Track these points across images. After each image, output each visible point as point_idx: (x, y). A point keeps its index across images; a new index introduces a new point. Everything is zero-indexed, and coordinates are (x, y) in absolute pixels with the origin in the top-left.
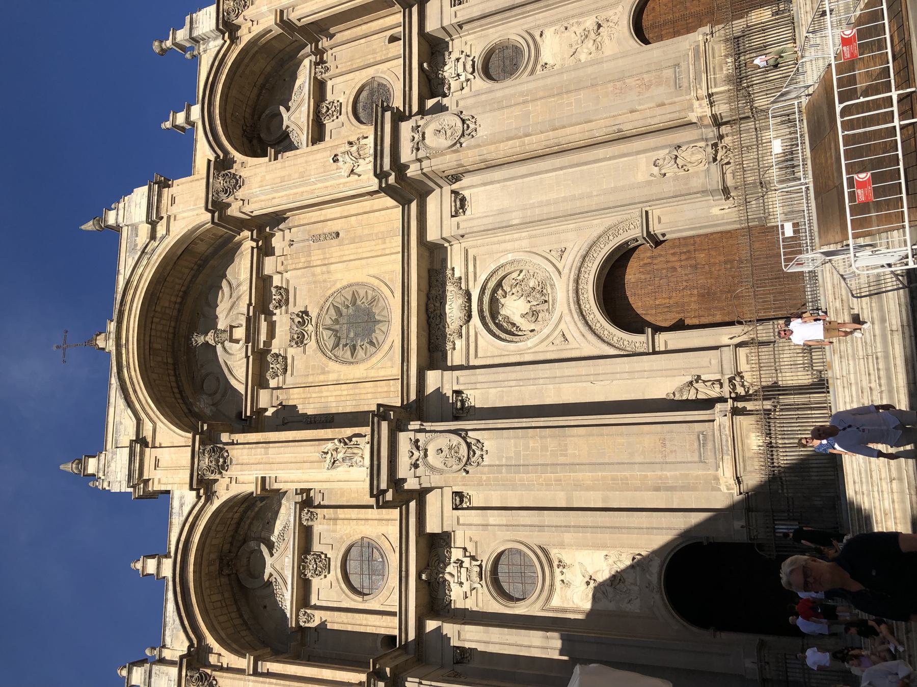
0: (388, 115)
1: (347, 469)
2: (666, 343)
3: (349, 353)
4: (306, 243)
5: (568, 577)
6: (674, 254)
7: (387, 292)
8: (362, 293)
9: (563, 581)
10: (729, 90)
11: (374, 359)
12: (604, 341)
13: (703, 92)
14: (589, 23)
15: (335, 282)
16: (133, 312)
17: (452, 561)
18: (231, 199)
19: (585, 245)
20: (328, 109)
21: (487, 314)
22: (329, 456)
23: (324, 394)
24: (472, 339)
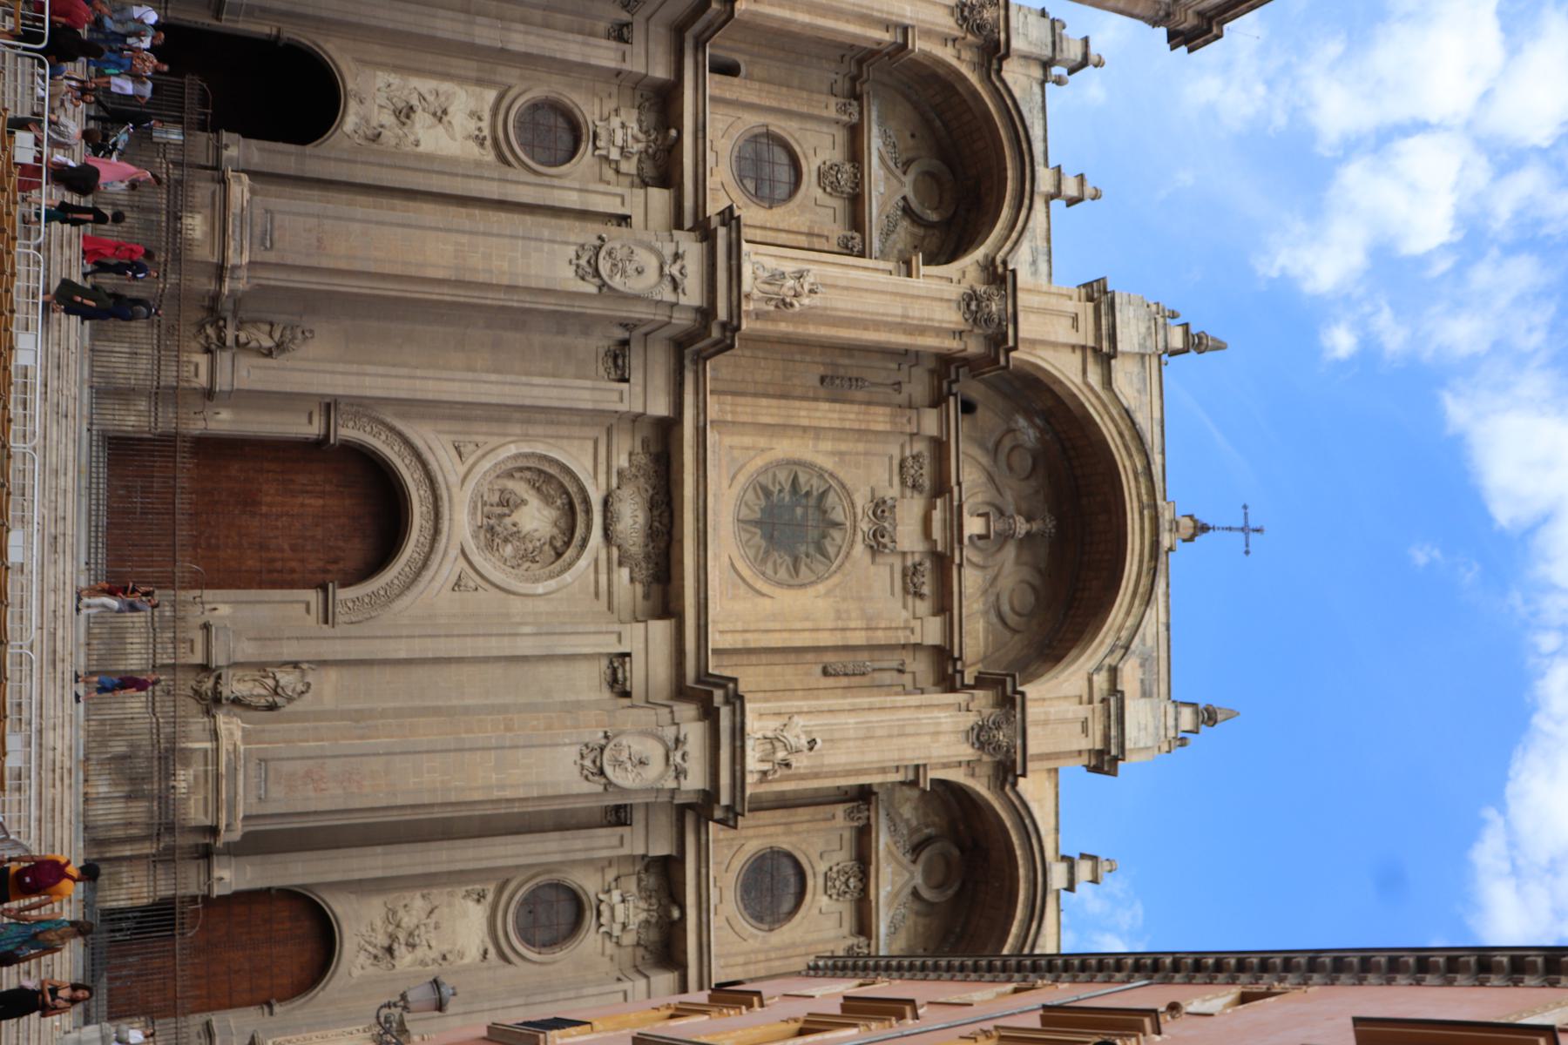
0: (725, 799)
1: (782, 269)
2: (310, 422)
3: (802, 479)
4: (877, 665)
5: (472, 125)
6: (293, 571)
7: (740, 566)
8: (783, 574)
9: (480, 119)
11: (759, 462)
12: (400, 435)
13: (225, 745)
14: (405, 958)
15: (828, 593)
17: (635, 159)
18: (987, 711)
20: (846, 883)
21: (579, 508)
22: (806, 287)
23: (836, 416)
24: (602, 468)
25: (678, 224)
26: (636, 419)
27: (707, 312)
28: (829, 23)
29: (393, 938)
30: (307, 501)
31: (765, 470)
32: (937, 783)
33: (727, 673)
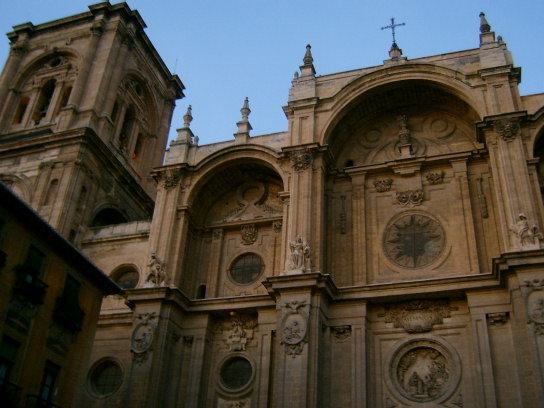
3: (392, 238)
16: (413, 74)
24: (394, 336)
25: (273, 307)
26: (368, 321)
27: (314, 290)
28: (178, 245)
32: (535, 156)
33: (491, 265)
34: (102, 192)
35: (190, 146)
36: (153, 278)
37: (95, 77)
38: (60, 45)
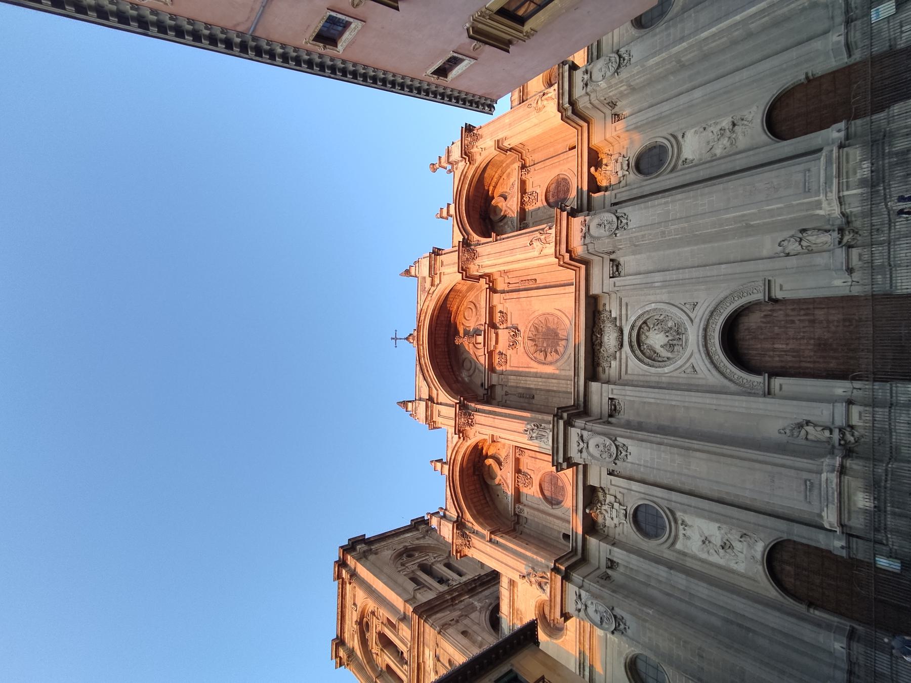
2: (781, 385)
5: (688, 532)
6: (793, 310)
8: (551, 318)
10: (862, 194)
12: (726, 378)
13: (833, 195)
14: (726, 123)
17: (607, 502)
19: (714, 303)
24: (623, 361)
26: (608, 382)
27: (568, 424)
29: (732, 131)
30: (784, 346)
31: (557, 361)
34: (474, 616)
35: (444, 517)
36: (543, 585)
37: (382, 594)
38: (355, 617)
